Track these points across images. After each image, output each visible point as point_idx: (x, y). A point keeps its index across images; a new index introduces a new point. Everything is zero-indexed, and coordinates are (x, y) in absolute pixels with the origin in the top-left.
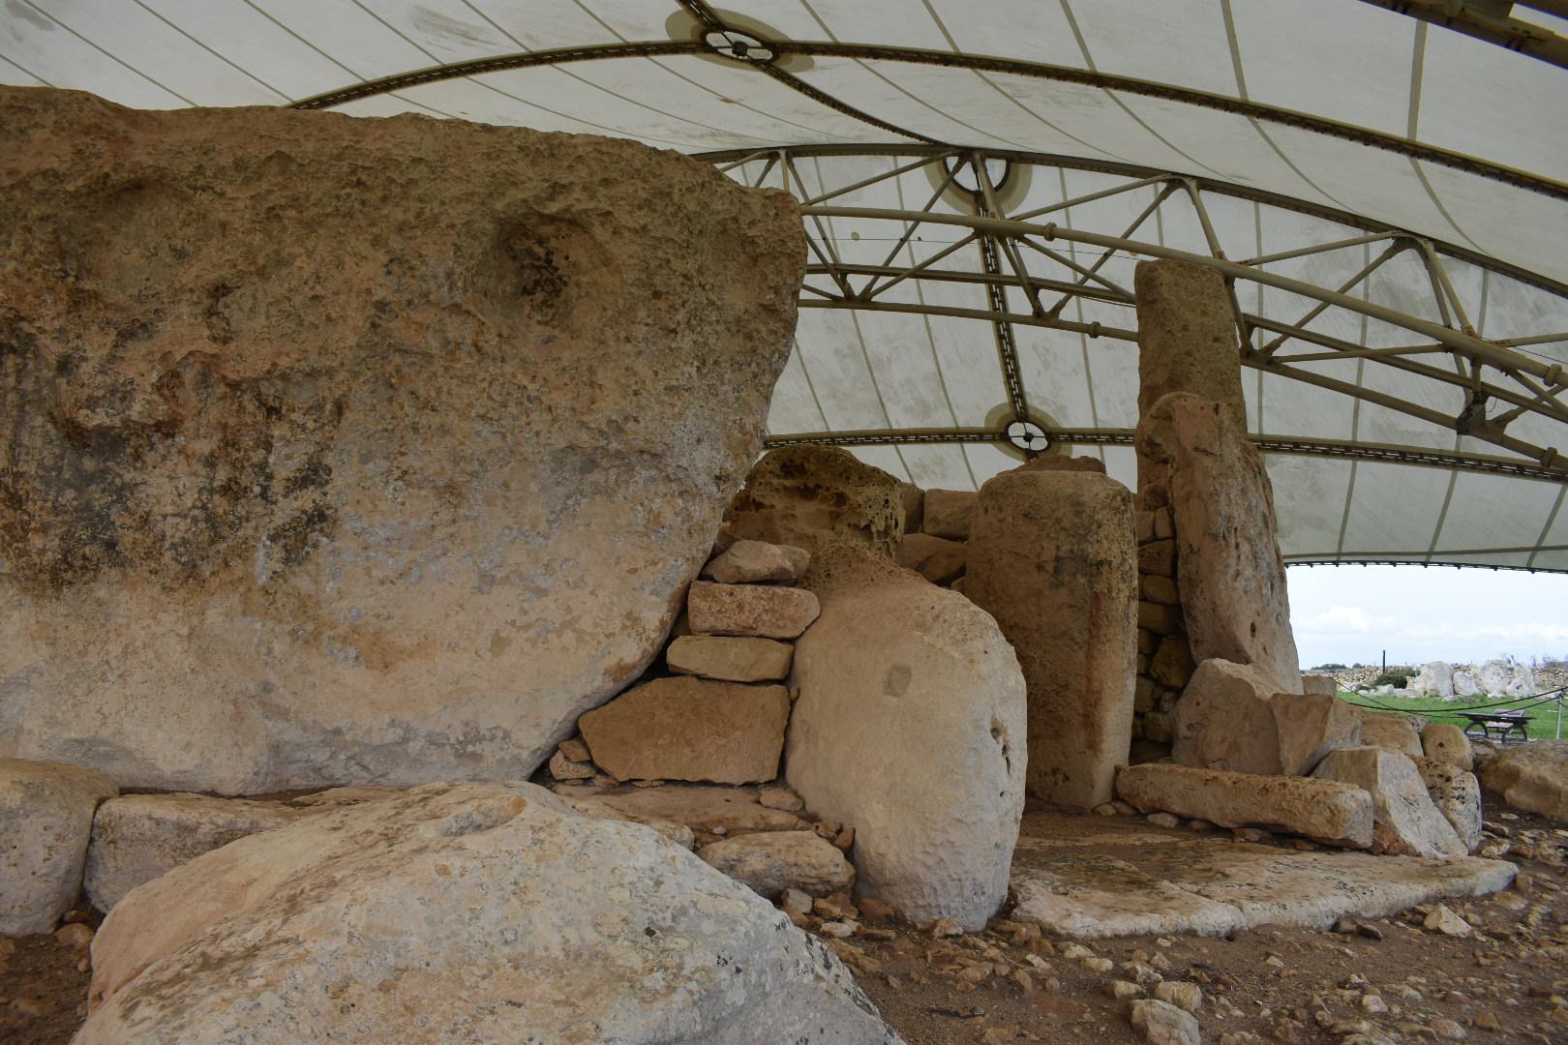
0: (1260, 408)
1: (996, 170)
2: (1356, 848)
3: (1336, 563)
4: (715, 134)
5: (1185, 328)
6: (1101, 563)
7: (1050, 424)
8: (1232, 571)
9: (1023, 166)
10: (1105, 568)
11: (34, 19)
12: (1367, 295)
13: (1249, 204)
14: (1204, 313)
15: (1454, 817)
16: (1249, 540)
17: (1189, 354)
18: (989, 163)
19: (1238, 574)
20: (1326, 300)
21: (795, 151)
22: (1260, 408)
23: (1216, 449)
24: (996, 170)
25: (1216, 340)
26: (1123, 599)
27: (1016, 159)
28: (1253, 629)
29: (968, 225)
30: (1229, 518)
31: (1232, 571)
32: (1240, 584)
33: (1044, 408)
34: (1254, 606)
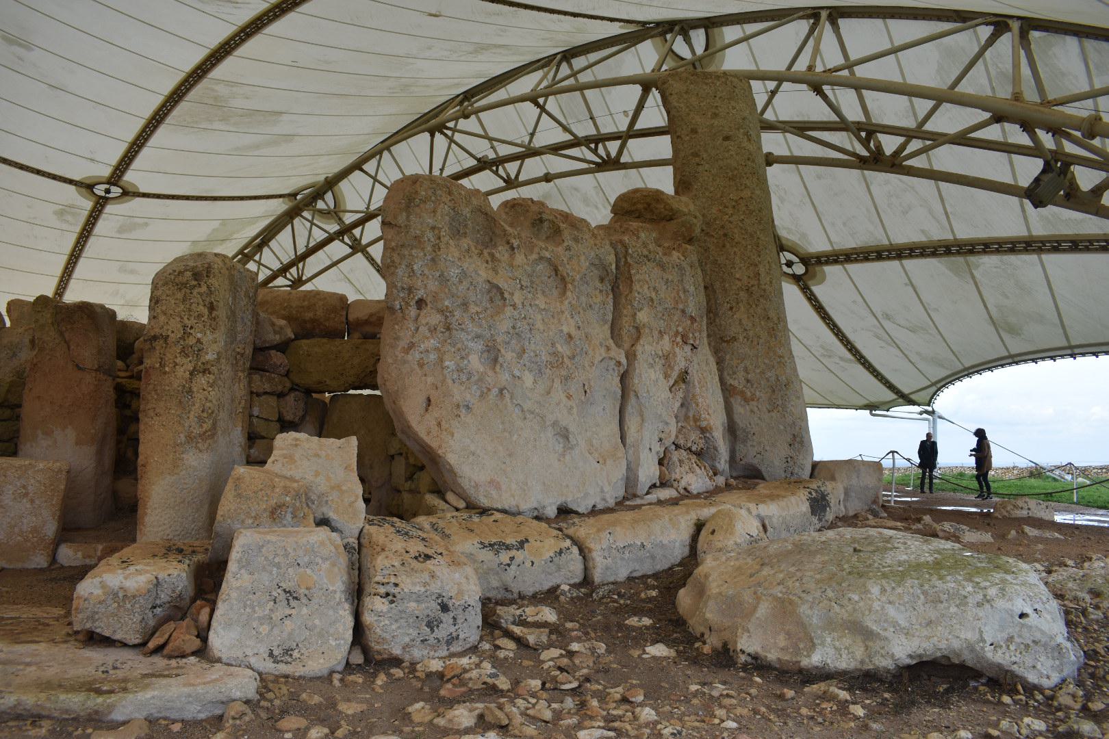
0: (946, 213)
1: (698, 37)
2: (125, 645)
3: (1073, 356)
4: (481, 48)
5: (694, 131)
6: (155, 338)
7: (801, 251)
8: (403, 344)
9: (716, 30)
10: (159, 344)
11: (20, 45)
12: (993, 89)
13: (878, 22)
14: (715, 115)
15: (368, 618)
16: (441, 311)
17: (696, 155)
18: (693, 33)
19: (412, 346)
20: (940, 98)
21: (568, 55)
22: (946, 213)
23: (401, 219)
24: (698, 37)
25: (727, 138)
26: (182, 372)
27: (710, 24)
28: (429, 400)
29: (634, 83)
30: (410, 290)
31: (403, 344)
32: (415, 355)
33: (791, 237)
34: (430, 380)
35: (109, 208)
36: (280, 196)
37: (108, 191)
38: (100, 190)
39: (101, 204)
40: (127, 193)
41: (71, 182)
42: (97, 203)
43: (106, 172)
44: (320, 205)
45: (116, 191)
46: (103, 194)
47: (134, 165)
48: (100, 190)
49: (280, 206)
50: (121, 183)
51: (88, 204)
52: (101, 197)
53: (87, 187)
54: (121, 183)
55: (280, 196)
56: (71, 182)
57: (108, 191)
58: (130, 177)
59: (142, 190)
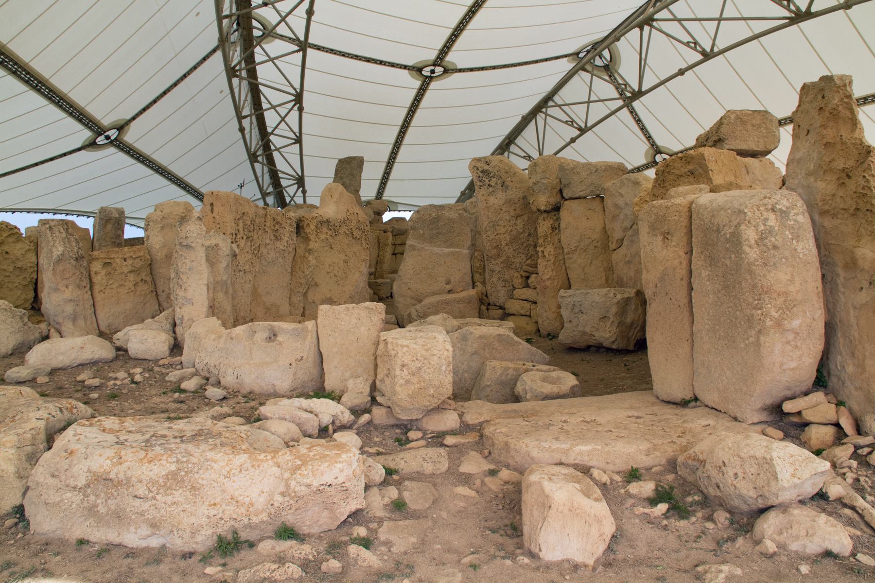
35: (433, 85)
36: (566, 56)
37: (433, 72)
38: (426, 72)
39: (426, 83)
40: (446, 71)
41: (405, 67)
42: (424, 81)
43: (432, 56)
44: (598, 62)
45: (439, 70)
46: (429, 74)
47: (456, 47)
48: (426, 72)
49: (566, 65)
50: (444, 64)
51: (417, 84)
52: (427, 77)
53: (418, 70)
54: (444, 64)
55: (566, 56)
56: (405, 67)
57: (433, 72)
58: (452, 58)
59: (459, 67)
